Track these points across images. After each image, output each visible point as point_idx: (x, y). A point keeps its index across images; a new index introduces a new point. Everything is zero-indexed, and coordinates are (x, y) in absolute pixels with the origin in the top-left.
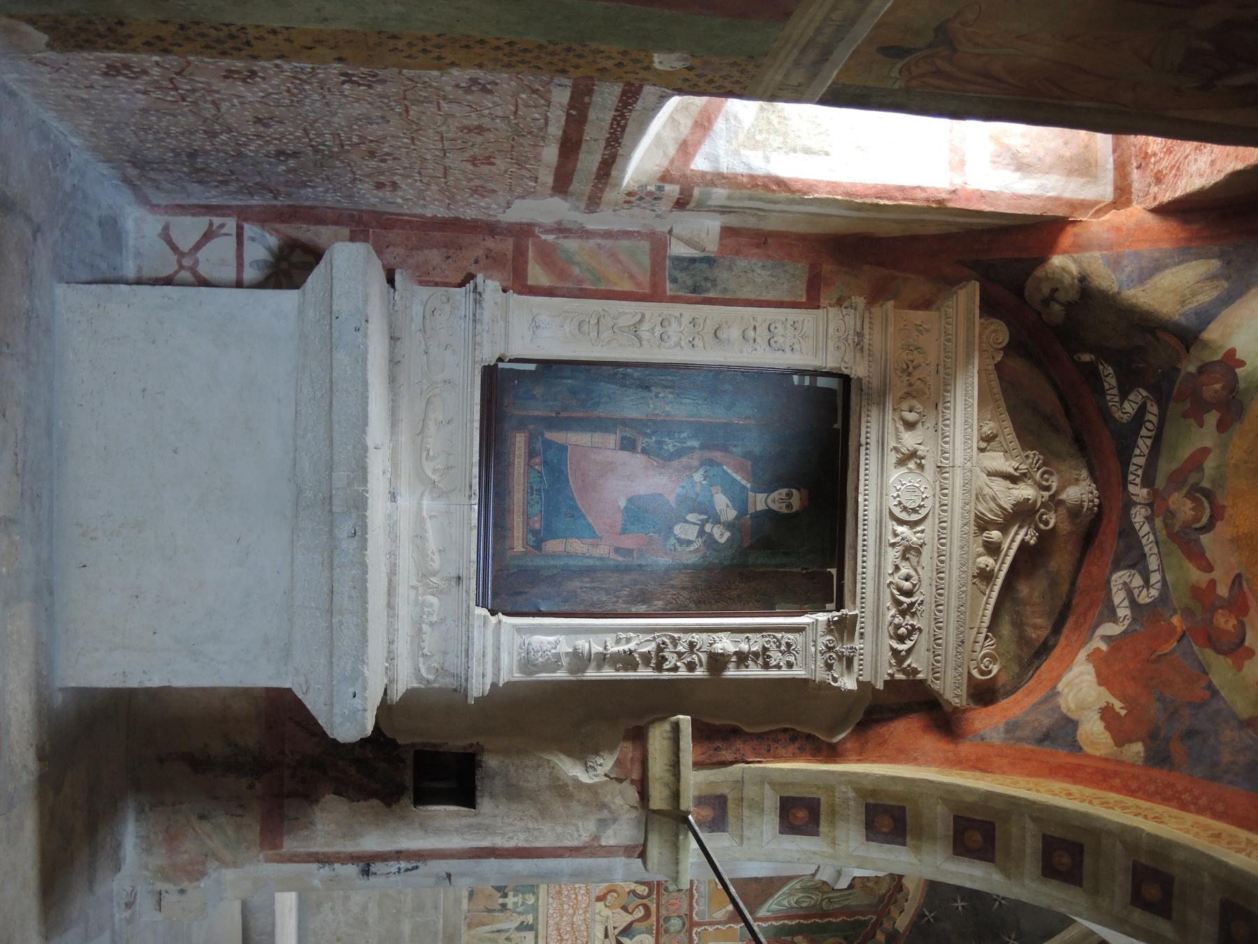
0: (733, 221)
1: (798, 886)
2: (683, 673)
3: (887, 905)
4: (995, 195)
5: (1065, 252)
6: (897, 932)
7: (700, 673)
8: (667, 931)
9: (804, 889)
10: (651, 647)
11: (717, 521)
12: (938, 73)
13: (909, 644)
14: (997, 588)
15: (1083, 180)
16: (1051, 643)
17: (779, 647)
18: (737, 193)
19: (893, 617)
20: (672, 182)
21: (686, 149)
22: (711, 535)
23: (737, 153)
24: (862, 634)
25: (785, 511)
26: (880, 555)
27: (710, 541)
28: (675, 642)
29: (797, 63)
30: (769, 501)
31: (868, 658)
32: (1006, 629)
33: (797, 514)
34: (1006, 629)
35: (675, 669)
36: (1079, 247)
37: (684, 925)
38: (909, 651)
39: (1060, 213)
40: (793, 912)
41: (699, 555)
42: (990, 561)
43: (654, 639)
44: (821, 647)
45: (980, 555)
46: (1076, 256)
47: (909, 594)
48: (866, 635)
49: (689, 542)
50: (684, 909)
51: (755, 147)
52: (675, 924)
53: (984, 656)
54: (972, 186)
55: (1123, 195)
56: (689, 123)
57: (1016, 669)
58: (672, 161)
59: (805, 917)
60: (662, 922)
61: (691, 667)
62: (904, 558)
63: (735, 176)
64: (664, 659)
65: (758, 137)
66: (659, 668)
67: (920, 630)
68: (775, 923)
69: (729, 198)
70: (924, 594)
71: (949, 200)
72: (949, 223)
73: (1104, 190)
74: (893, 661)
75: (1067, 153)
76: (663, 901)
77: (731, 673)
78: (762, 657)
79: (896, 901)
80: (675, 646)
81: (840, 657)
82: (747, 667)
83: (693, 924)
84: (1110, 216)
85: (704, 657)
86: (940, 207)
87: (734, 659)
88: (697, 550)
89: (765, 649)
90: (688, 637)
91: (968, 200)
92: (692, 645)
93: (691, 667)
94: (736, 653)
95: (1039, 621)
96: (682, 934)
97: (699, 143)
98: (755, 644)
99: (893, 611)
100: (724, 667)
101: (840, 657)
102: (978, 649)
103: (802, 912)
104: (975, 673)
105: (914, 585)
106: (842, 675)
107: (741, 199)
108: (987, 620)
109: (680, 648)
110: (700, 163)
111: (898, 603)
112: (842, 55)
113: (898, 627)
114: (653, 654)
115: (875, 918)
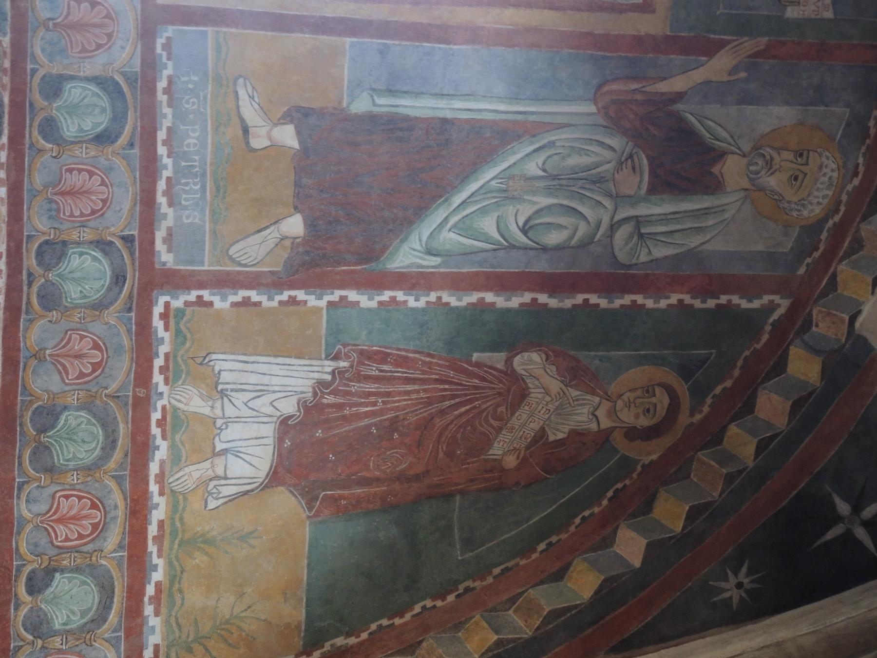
1: (533, 168)
3: (829, 257)
6: (863, 342)
8: (51, 299)
9: (555, 181)
37: (119, 279)
40: (513, 264)
50: (121, 218)
52: (85, 273)
59: (554, 284)
60: (30, 261)
68: (450, 299)
76: (39, 175)
79: (858, 245)
83: (155, 280)
96: (111, 316)
103: (541, 265)
115: (783, 304)
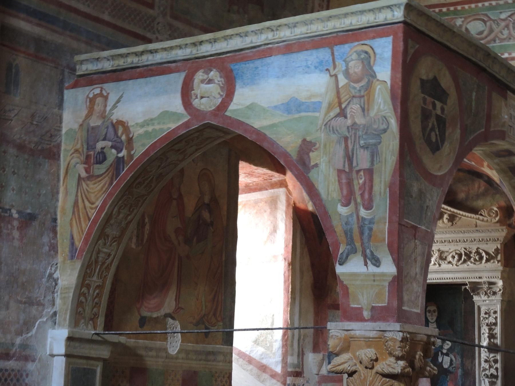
0: (309, 346)
2: (499, 365)
4: (286, 241)
5: (307, 206)
7: (499, 357)
10: (487, 380)
11: (442, 347)
12: (215, 315)
13: (484, 254)
14: (459, 212)
15: (279, 202)
16: (486, 179)
17: (487, 318)
18: (290, 352)
19: (471, 262)
20: (286, 381)
21: (274, 375)
22: (448, 350)
23: (274, 354)
24: (480, 278)
25: (436, 313)
26: (443, 272)
27: (450, 350)
28: (485, 370)
29: (214, 360)
30: (432, 321)
31: (490, 274)
32: (480, 203)
33: (438, 308)
34: (480, 203)
35: (497, 369)
36: (303, 200)
38: (487, 253)
39: (291, 211)
41: (457, 356)
42: (446, 216)
43: (483, 380)
44: (486, 298)
45: (443, 222)
46: (307, 202)
47: (460, 256)
48: (480, 276)
49: (451, 360)
51: (271, 346)
53: (490, 216)
54: (283, 251)
55: (283, 184)
56: (264, 374)
57: (498, 196)
58: (278, 381)
61: (496, 361)
62: (445, 259)
63: (283, 354)
64: (492, 375)
65: (268, 345)
66: (496, 377)
67: (478, 248)
69: (292, 355)
70: (461, 248)
71: (288, 261)
72: (302, 254)
73: (281, 191)
74: (492, 261)
75: (269, 211)
77: (498, 341)
78: (491, 326)
80: (487, 369)
81: (490, 288)
82: (496, 334)
84: (290, 187)
85: (492, 355)
86: (292, 265)
87: (492, 340)
88: (455, 357)
89: (487, 325)
90: (483, 364)
91: (288, 252)
92: (486, 361)
93: (496, 361)
94: (490, 340)
95: (476, 186)
97: (272, 370)
98: (485, 330)
99: (469, 263)
100: (496, 345)
101: (490, 288)
102: (485, 219)
104: (497, 219)
105: (456, 253)
106: (498, 287)
107: (293, 350)
108: (473, 215)
109: (487, 367)
110: (278, 369)
111: (465, 261)
112: (210, 347)
113: (475, 260)
114: (490, 380)
